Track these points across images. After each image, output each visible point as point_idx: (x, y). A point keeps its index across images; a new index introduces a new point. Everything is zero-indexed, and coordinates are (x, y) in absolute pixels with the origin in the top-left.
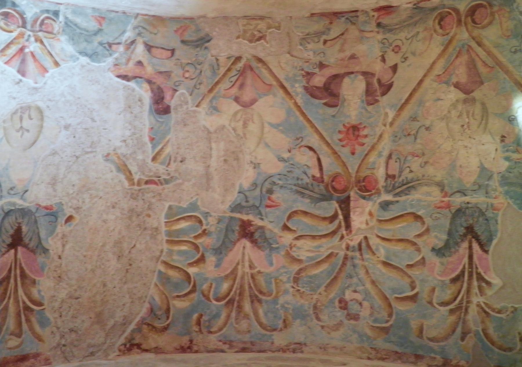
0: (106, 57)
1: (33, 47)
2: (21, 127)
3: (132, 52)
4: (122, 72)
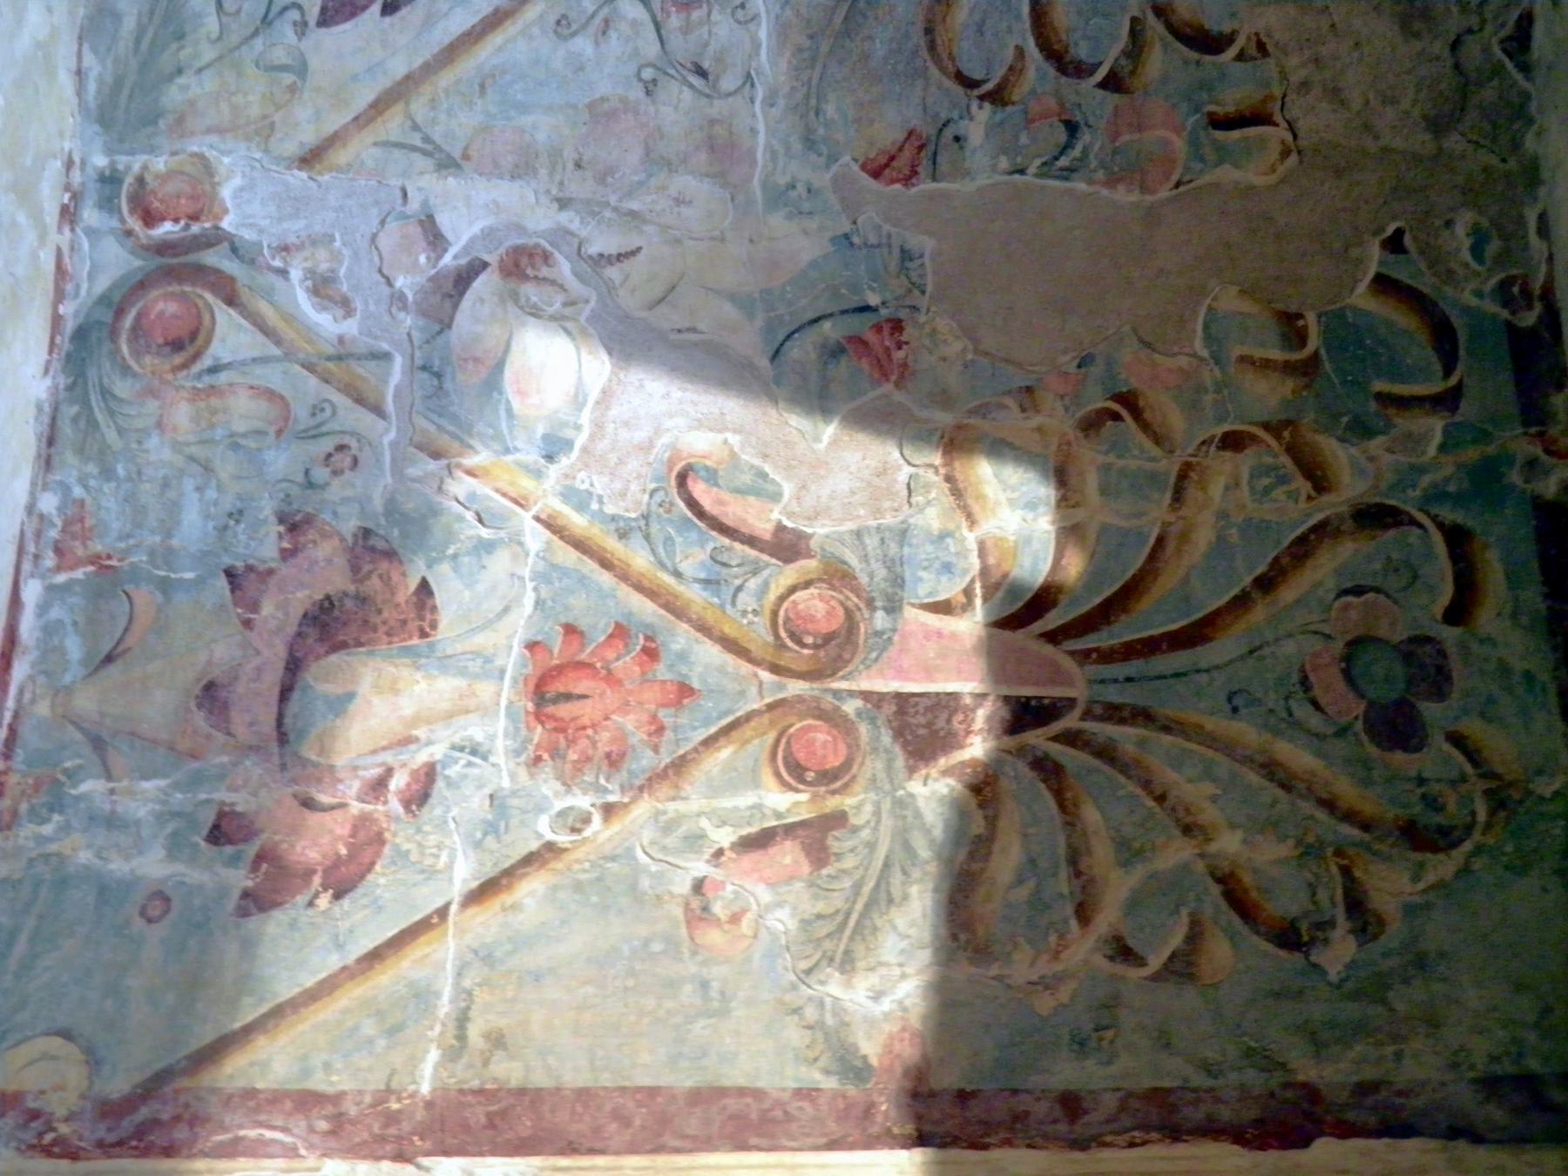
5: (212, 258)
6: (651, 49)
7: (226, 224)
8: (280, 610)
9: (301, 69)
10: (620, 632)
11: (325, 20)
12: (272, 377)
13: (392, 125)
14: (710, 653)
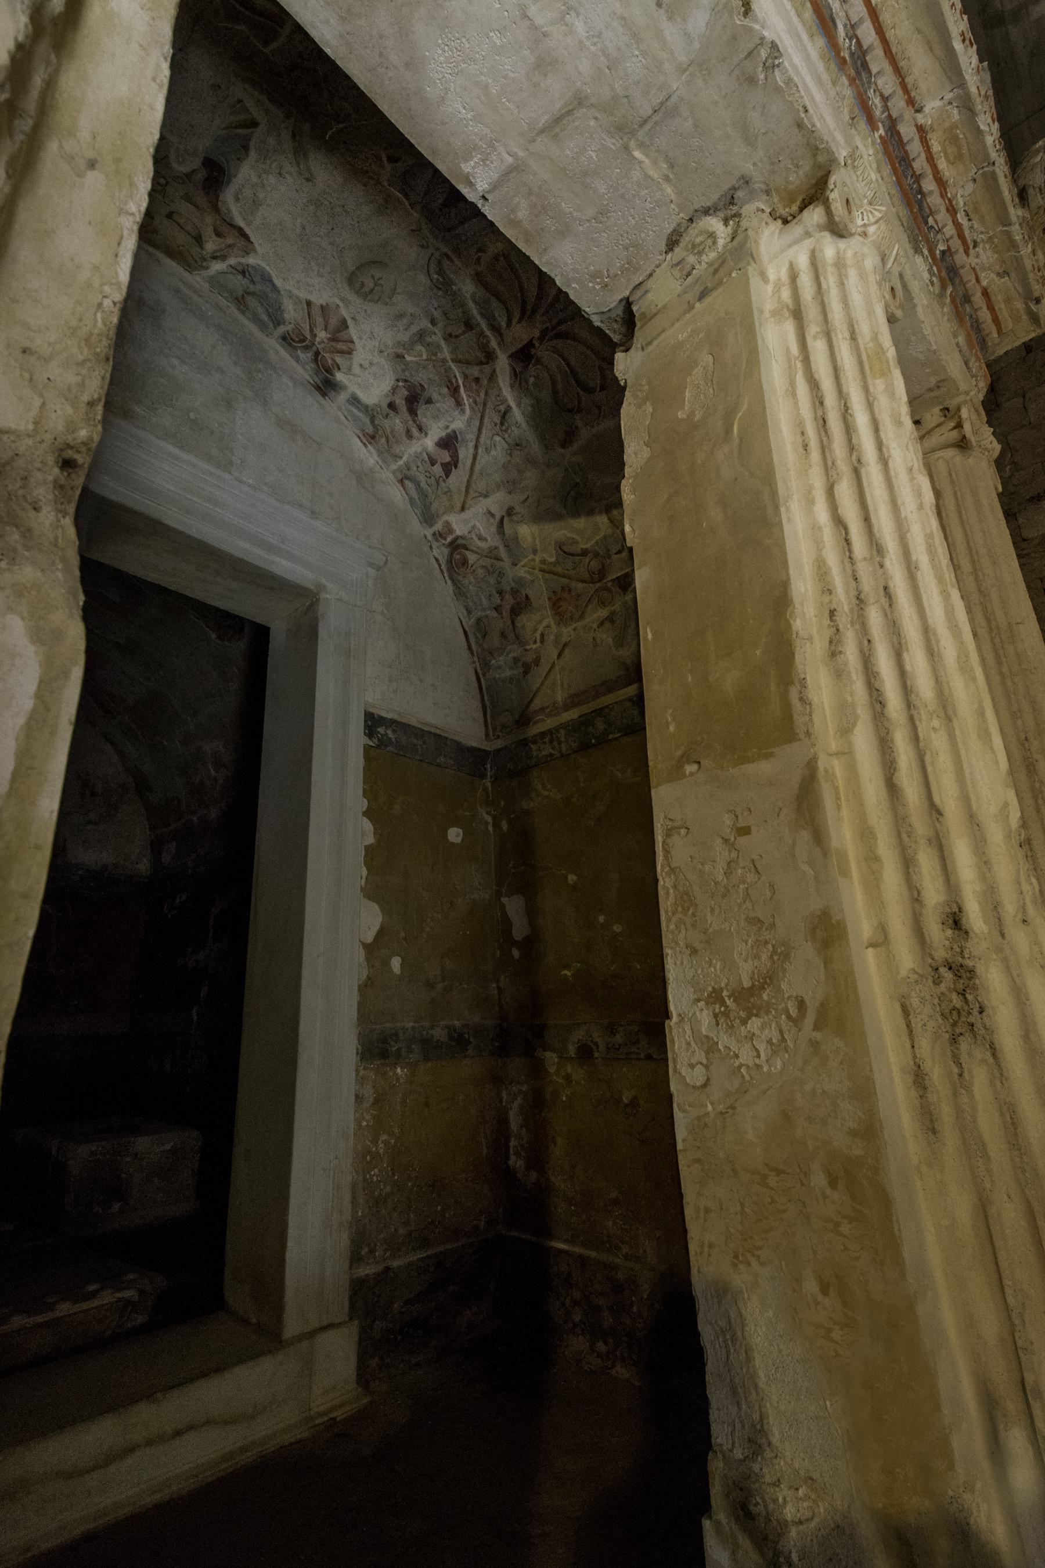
0: (253, 267)
1: (322, 335)
2: (376, 285)
3: (221, 250)
4: (242, 242)
5: (460, 541)
6: (506, 445)
7: (458, 533)
8: (506, 613)
9: (449, 491)
10: (563, 588)
11: (447, 477)
12: (481, 562)
13: (472, 494)
14: (580, 585)
